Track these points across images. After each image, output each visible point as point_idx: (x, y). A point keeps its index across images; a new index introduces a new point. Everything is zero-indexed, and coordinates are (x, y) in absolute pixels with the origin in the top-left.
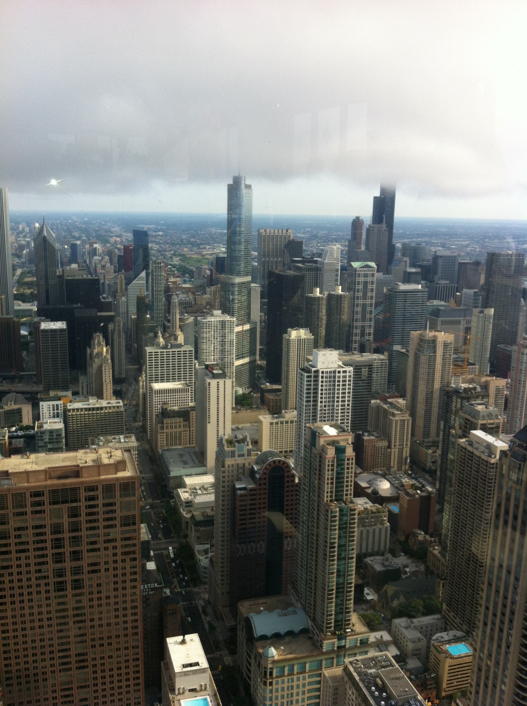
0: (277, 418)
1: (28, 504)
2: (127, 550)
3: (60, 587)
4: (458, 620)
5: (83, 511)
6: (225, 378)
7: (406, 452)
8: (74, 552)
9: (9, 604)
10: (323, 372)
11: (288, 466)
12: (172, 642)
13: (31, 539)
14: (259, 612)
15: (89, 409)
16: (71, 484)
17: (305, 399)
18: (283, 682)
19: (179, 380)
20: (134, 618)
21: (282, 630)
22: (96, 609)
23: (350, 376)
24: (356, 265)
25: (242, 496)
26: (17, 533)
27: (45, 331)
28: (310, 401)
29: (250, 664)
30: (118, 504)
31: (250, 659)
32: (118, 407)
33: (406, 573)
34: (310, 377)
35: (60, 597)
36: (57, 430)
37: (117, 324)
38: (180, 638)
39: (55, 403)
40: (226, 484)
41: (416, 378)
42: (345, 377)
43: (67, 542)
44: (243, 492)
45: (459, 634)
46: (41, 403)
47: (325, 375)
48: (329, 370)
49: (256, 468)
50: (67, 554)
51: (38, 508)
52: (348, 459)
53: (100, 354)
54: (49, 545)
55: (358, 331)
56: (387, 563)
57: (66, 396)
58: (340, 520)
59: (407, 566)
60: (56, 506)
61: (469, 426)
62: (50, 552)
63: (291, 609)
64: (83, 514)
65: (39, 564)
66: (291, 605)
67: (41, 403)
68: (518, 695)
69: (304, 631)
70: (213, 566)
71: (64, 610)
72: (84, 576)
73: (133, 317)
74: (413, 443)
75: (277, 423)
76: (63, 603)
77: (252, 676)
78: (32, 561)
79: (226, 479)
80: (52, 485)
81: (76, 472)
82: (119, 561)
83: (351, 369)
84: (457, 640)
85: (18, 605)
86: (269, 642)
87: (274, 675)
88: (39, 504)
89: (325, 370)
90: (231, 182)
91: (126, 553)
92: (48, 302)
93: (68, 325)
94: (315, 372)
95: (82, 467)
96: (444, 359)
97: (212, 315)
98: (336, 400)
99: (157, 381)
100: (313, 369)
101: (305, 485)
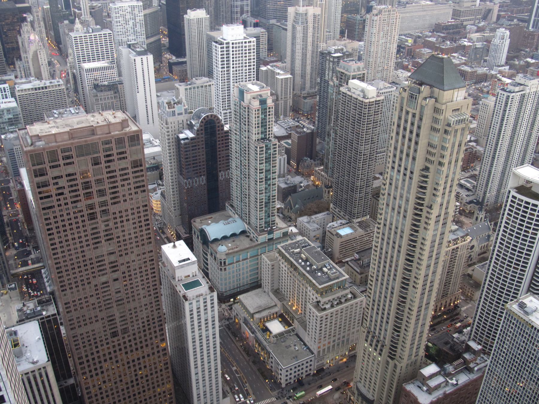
0: (190, 85)
1: (60, 158)
2: (138, 185)
3: (92, 216)
4: (342, 214)
5: (103, 160)
6: (147, 54)
7: (290, 102)
8: (100, 191)
9: (55, 234)
10: (233, 44)
11: (218, 119)
12: (167, 248)
13: (66, 184)
14: (208, 224)
15: (36, 89)
16: (92, 140)
17: (220, 66)
18: (233, 268)
19: (103, 59)
20: (148, 232)
21: (228, 235)
22: (120, 229)
23: (254, 46)
25: (185, 144)
26: (55, 181)
29: (207, 260)
30: (128, 152)
31: (207, 255)
32: (59, 85)
33: (301, 187)
34: (223, 48)
35: (93, 224)
36: (13, 108)
37: (35, 14)
38: (172, 244)
40: (171, 137)
41: (293, 44)
43: (93, 184)
44: (186, 141)
45: (344, 221)
47: (234, 46)
48: (237, 41)
50: (95, 193)
51: (68, 161)
52: (269, 108)
53: (30, 42)
54: (80, 187)
55: (239, 9)
56: (289, 182)
57: (10, 80)
58: (266, 153)
59: (301, 183)
60: (82, 158)
61: (344, 78)
62: (81, 192)
63: (230, 219)
64: (103, 162)
65: (75, 202)
66: (230, 217)
68: (410, 245)
69: (243, 232)
70: (165, 198)
71: (97, 233)
72: (109, 207)
73: (45, 7)
74: (294, 95)
76: (96, 228)
77: (209, 267)
78: (69, 201)
79: (170, 133)
80: (77, 142)
81: (92, 130)
82: (133, 194)
83: (255, 39)
84: (342, 225)
85: (62, 234)
86: (220, 242)
87: (227, 264)
88: (68, 157)
89: (234, 42)
91: (138, 187)
95: (96, 127)
96: (314, 28)
99: (84, 61)
100: (225, 42)
101: (236, 130)
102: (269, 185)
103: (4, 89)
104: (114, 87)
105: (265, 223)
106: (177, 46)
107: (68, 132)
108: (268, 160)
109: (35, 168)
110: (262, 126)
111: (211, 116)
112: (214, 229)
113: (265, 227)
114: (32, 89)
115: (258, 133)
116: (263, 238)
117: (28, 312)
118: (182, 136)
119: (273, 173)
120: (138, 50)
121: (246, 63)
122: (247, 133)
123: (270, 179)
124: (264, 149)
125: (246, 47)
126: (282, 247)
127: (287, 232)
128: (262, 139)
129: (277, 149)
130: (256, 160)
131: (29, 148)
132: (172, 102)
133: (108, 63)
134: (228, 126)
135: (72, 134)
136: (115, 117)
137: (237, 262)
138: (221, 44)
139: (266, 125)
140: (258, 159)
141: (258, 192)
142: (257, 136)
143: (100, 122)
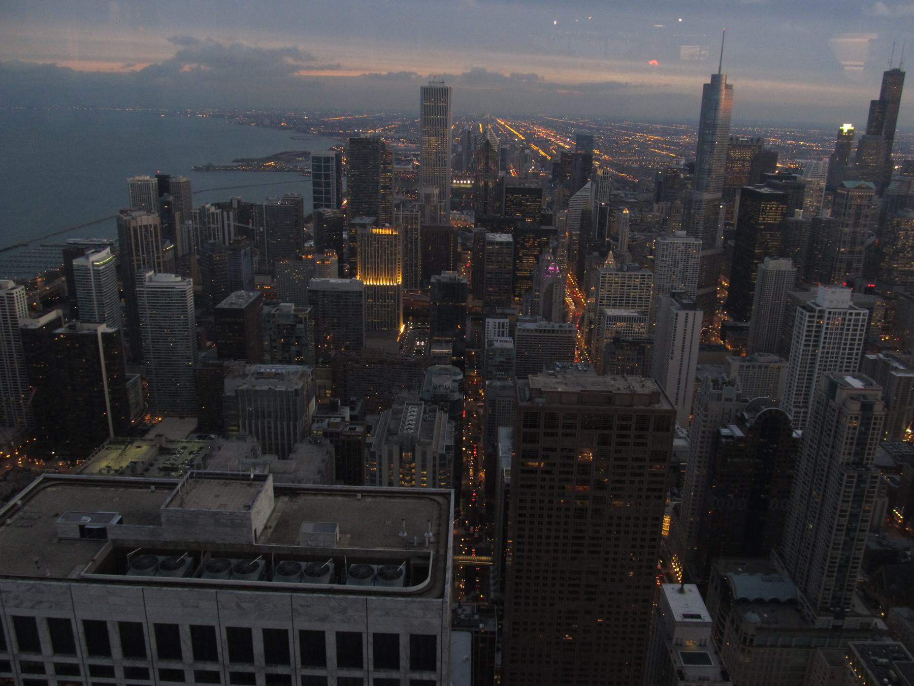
0: (749, 361)
6: (695, 310)
10: (830, 313)
11: (786, 418)
14: (738, 573)
15: (540, 331)
17: (803, 343)
19: (633, 307)
23: (864, 320)
24: (848, 184)
27: (492, 243)
28: (809, 345)
29: (724, 627)
31: (725, 619)
32: (570, 331)
33: (906, 556)
34: (813, 317)
36: (508, 350)
39: (502, 320)
42: (857, 320)
44: (729, 440)
46: (487, 320)
47: (832, 316)
49: (746, 416)
51: (569, 431)
56: (884, 543)
57: (513, 314)
58: (858, 486)
59: (908, 549)
66: (775, 571)
67: (487, 320)
69: (792, 602)
75: (748, 367)
81: (609, 398)
83: (867, 311)
87: (755, 643)
88: (570, 426)
90: (709, 81)
91: (652, 490)
92: (485, 212)
93: (514, 236)
94: (820, 311)
97: (675, 236)
98: (842, 346)
99: (608, 305)
100: (818, 308)
101: (812, 441)
102: (852, 539)
103: (503, 324)
104: (639, 347)
105: (834, 597)
106: (739, 303)
107: (578, 393)
108: (858, 498)
109: (526, 430)
110: (857, 444)
111: (777, 411)
112: (745, 584)
113: (831, 606)
114: (536, 330)
115: (850, 454)
116: (824, 621)
117: (462, 617)
118: (725, 431)
119: (863, 521)
120: (684, 301)
121: (845, 344)
122: (829, 449)
123: (855, 529)
124: (855, 480)
125: (850, 320)
126: (855, 646)
127: (869, 624)
128: (853, 463)
129: (877, 485)
130: (839, 494)
131: (526, 404)
132: (720, 382)
133: (639, 312)
134: (800, 432)
135: (582, 397)
136: (643, 386)
137: (772, 646)
138: (812, 310)
139: (865, 444)
140: (842, 493)
141: (831, 545)
142: (846, 457)
143: (621, 387)
